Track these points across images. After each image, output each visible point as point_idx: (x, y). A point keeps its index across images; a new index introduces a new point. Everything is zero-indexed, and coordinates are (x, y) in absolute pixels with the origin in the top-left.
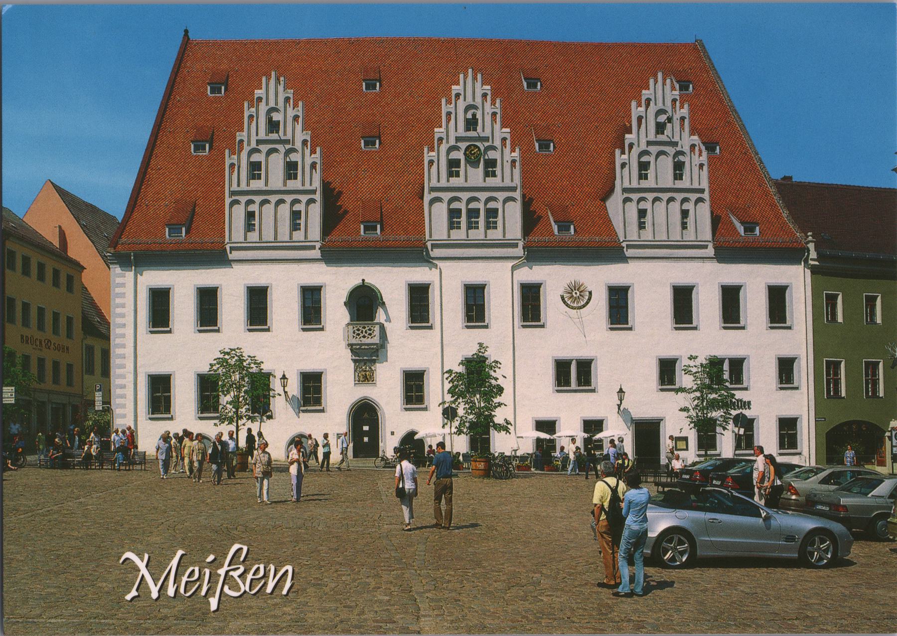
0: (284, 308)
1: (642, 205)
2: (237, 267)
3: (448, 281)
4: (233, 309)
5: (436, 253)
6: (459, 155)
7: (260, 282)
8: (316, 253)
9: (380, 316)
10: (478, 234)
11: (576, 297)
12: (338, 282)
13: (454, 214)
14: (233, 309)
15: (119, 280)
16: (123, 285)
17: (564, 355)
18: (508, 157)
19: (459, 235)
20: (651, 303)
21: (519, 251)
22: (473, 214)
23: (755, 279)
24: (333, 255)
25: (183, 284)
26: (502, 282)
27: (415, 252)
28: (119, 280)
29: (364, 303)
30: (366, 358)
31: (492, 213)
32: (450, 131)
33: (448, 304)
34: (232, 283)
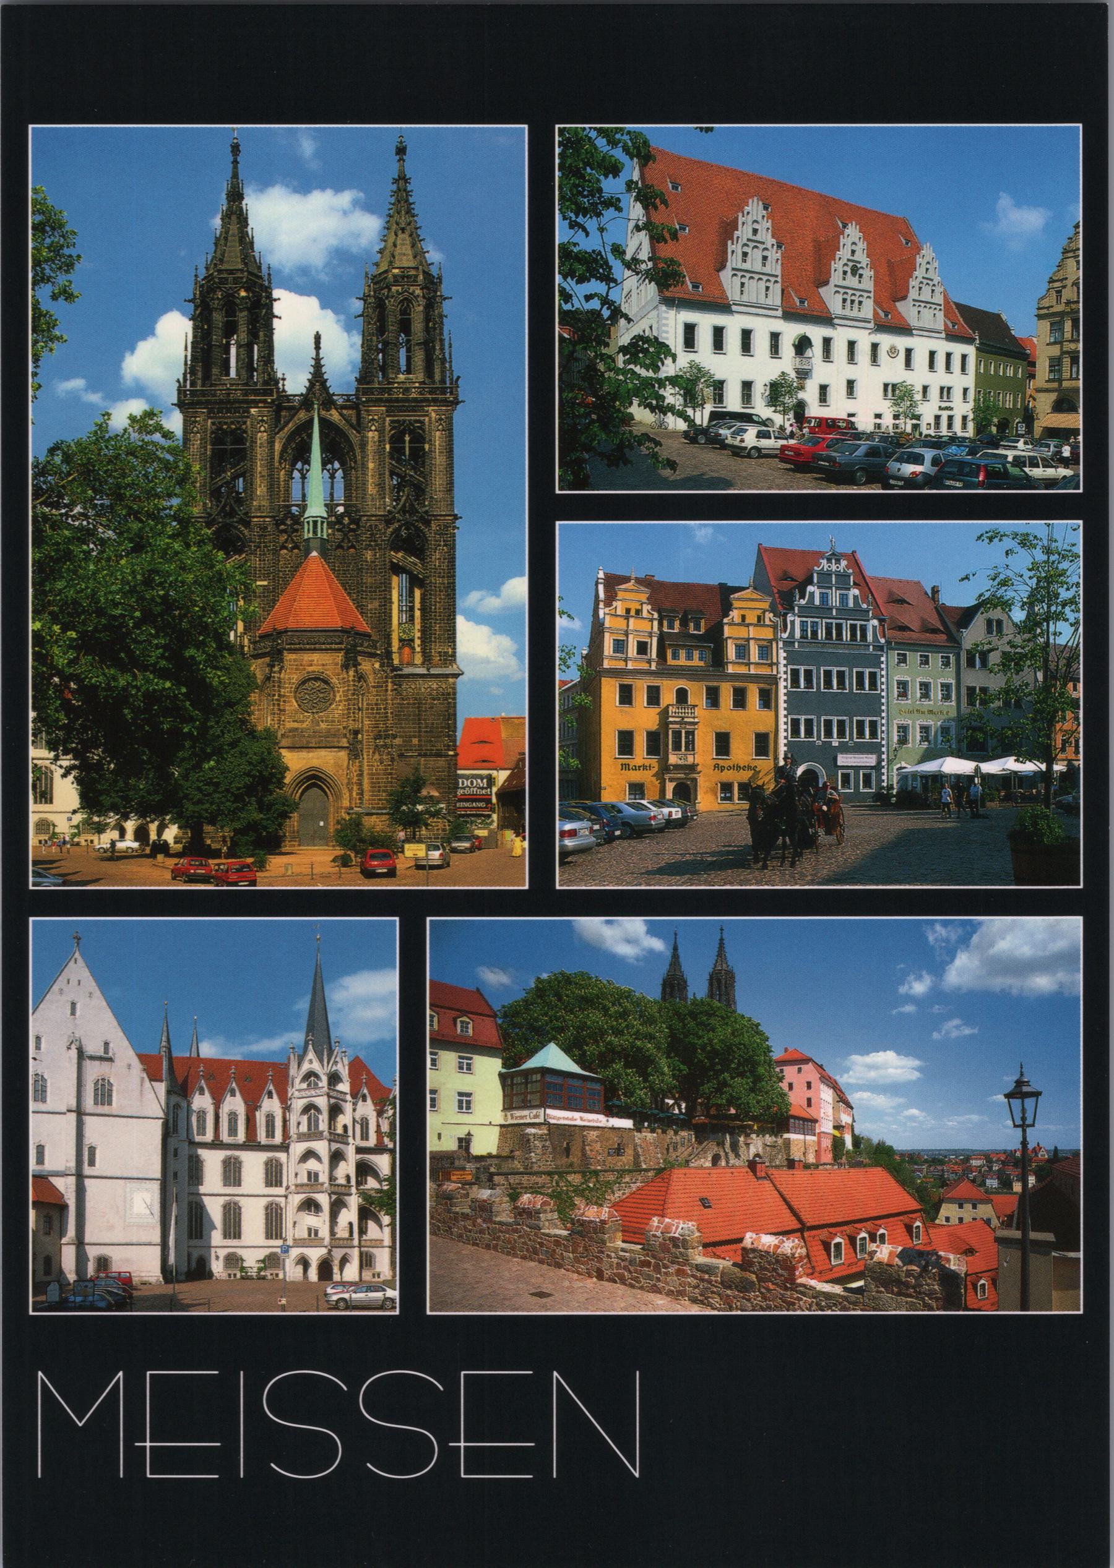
0: (761, 343)
1: (743, 280)
2: (737, 316)
3: (840, 336)
4: (733, 340)
5: (836, 321)
6: (848, 269)
7: (748, 326)
8: (779, 313)
9: (809, 353)
10: (855, 313)
11: (893, 352)
12: (791, 331)
13: (844, 300)
14: (733, 340)
15: (664, 315)
16: (667, 319)
17: (887, 381)
18: (868, 273)
19: (847, 312)
20: (920, 359)
21: (871, 325)
22: (852, 302)
23: (958, 349)
24: (790, 315)
25: (705, 322)
26: (864, 339)
27: (826, 320)
28: (664, 315)
29: (802, 345)
30: (803, 374)
31: (860, 303)
32: (844, 254)
33: (839, 349)
34: (733, 325)
